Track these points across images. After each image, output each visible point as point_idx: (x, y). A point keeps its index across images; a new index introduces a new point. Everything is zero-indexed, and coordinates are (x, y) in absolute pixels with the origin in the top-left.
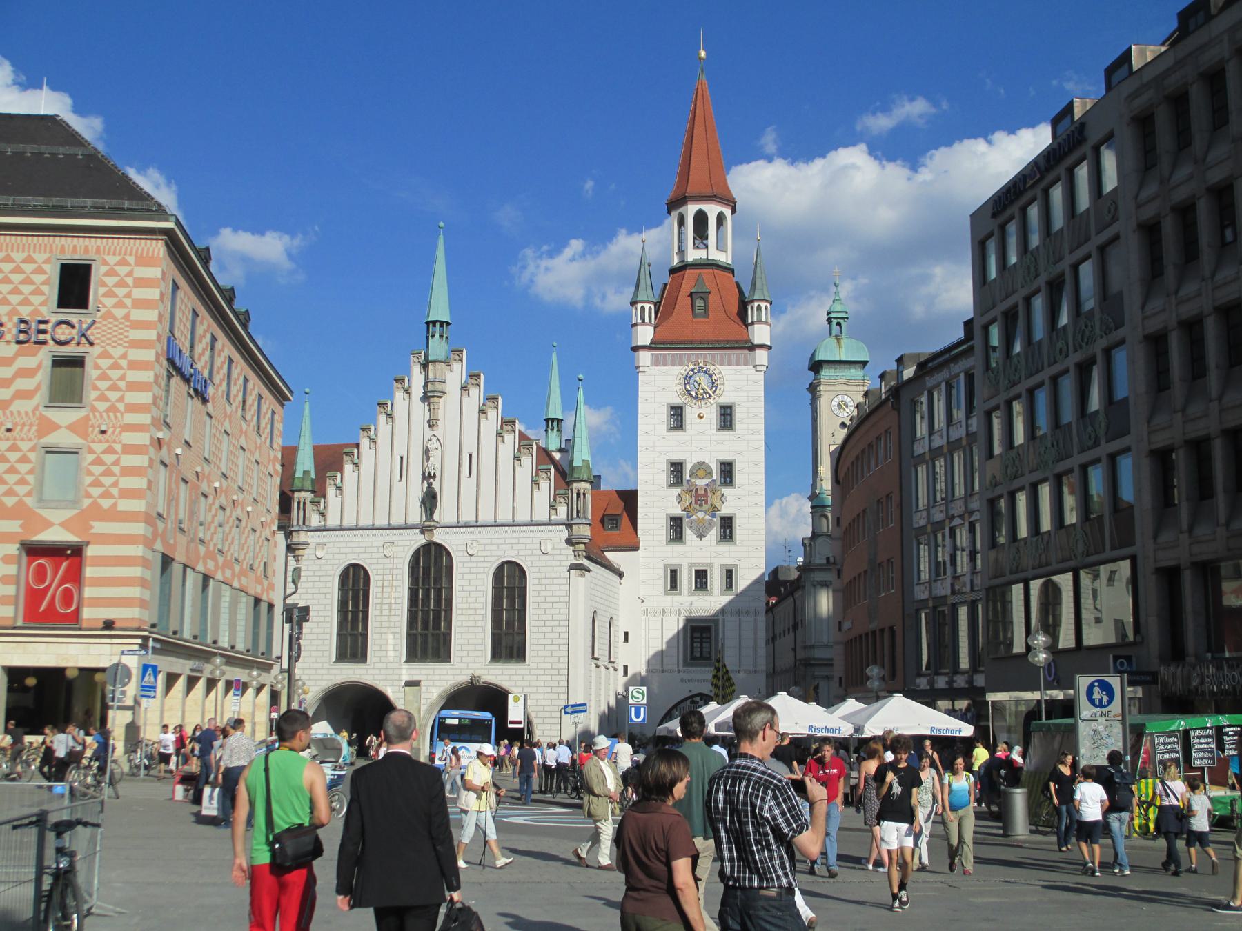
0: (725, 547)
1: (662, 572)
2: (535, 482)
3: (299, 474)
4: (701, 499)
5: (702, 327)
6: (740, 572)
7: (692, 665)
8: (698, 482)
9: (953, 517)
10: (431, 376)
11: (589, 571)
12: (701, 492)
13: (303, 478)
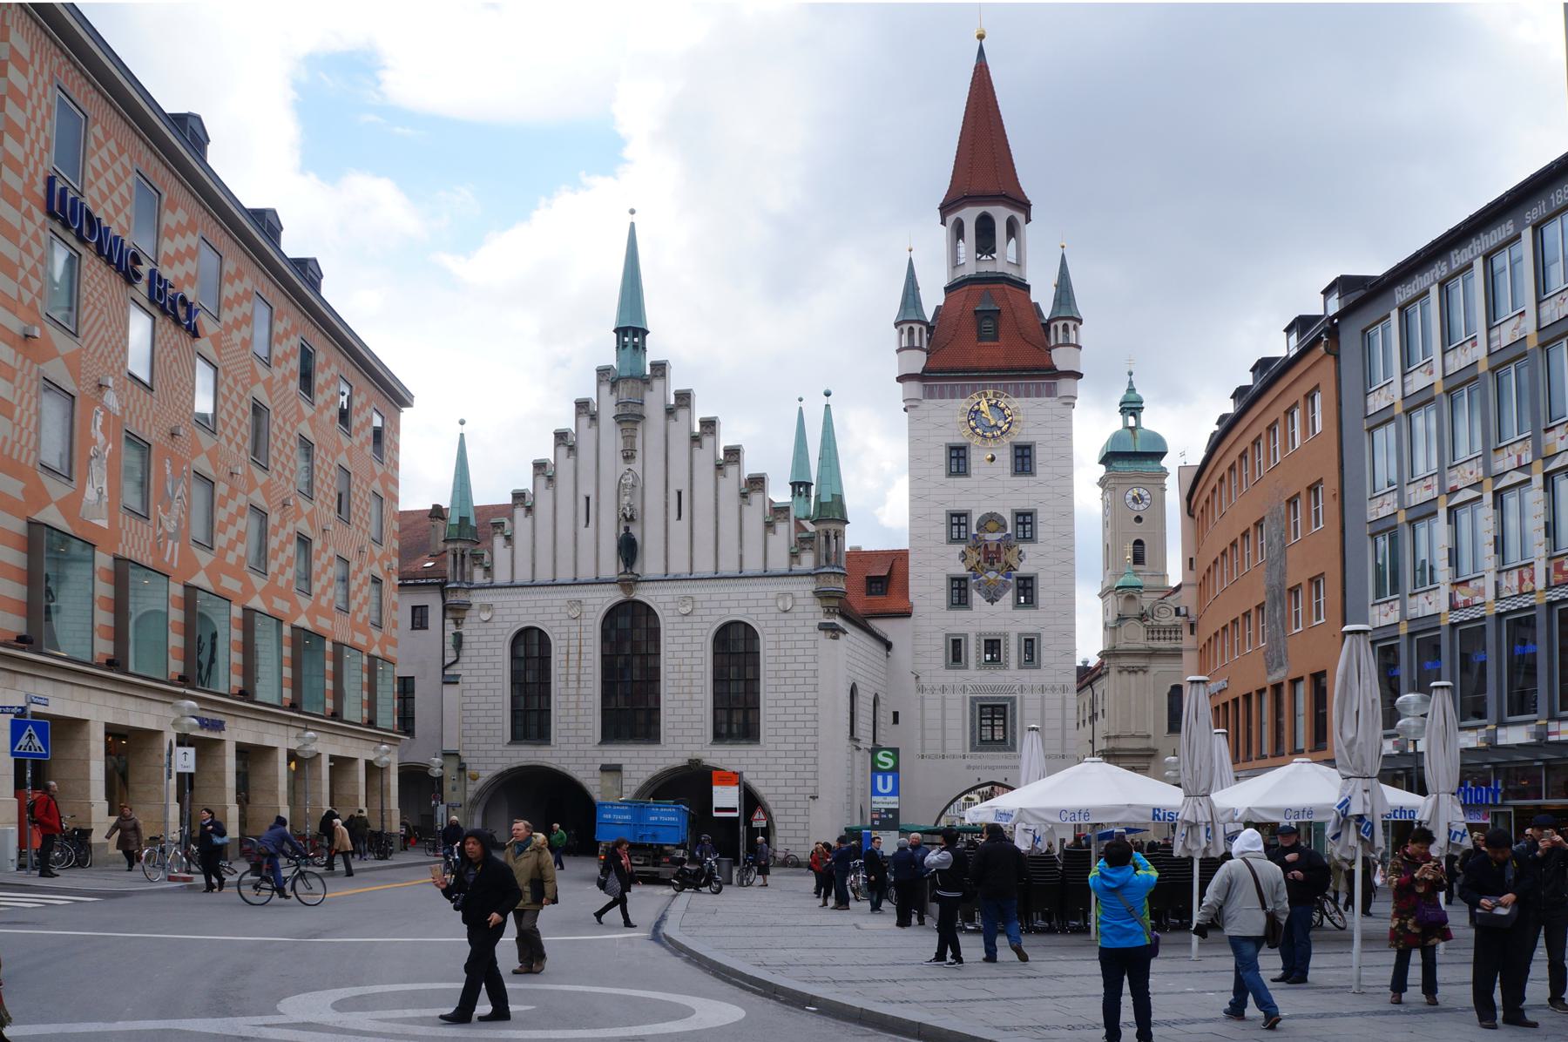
2: (769, 526)
4: (991, 556)
8: (988, 537)
9: (1455, 491)
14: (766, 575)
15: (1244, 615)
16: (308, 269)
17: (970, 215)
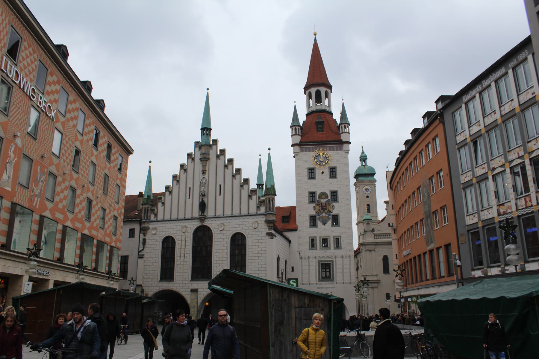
0: (334, 229)
1: (308, 240)
2: (250, 197)
4: (323, 208)
5: (322, 136)
6: (342, 239)
7: (322, 281)
9: (494, 169)
11: (275, 236)
12: (324, 205)
14: (249, 215)
15: (416, 224)
16: (101, 103)
17: (313, 90)
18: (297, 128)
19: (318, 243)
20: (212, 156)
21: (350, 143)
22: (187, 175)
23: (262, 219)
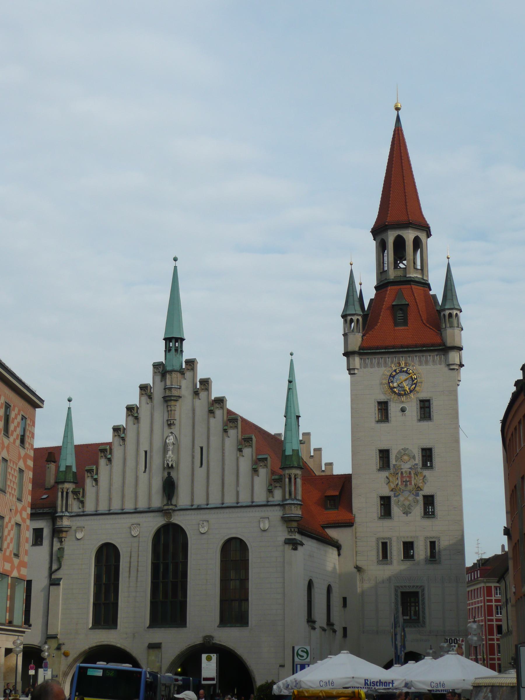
0: (428, 523)
2: (255, 471)
3: (63, 468)
5: (404, 334)
10: (168, 383)
13: (66, 472)
14: (252, 506)
18: (355, 318)
19: (396, 551)
20: (186, 391)
21: (461, 349)
22: (138, 427)
23: (276, 513)
